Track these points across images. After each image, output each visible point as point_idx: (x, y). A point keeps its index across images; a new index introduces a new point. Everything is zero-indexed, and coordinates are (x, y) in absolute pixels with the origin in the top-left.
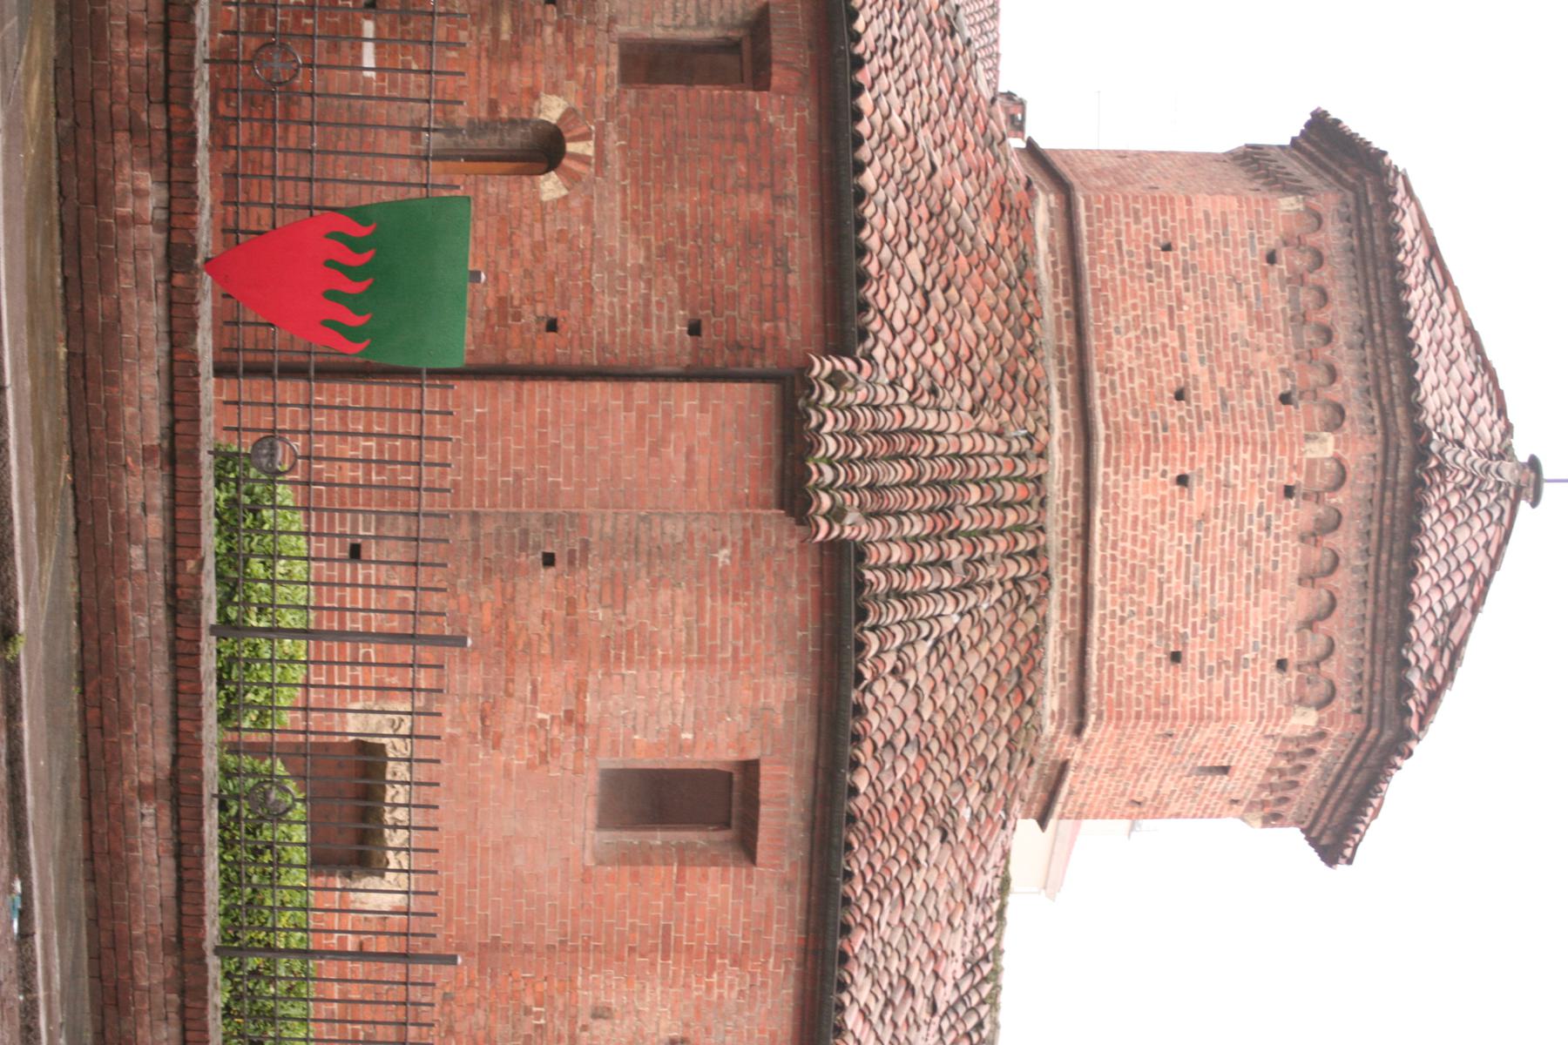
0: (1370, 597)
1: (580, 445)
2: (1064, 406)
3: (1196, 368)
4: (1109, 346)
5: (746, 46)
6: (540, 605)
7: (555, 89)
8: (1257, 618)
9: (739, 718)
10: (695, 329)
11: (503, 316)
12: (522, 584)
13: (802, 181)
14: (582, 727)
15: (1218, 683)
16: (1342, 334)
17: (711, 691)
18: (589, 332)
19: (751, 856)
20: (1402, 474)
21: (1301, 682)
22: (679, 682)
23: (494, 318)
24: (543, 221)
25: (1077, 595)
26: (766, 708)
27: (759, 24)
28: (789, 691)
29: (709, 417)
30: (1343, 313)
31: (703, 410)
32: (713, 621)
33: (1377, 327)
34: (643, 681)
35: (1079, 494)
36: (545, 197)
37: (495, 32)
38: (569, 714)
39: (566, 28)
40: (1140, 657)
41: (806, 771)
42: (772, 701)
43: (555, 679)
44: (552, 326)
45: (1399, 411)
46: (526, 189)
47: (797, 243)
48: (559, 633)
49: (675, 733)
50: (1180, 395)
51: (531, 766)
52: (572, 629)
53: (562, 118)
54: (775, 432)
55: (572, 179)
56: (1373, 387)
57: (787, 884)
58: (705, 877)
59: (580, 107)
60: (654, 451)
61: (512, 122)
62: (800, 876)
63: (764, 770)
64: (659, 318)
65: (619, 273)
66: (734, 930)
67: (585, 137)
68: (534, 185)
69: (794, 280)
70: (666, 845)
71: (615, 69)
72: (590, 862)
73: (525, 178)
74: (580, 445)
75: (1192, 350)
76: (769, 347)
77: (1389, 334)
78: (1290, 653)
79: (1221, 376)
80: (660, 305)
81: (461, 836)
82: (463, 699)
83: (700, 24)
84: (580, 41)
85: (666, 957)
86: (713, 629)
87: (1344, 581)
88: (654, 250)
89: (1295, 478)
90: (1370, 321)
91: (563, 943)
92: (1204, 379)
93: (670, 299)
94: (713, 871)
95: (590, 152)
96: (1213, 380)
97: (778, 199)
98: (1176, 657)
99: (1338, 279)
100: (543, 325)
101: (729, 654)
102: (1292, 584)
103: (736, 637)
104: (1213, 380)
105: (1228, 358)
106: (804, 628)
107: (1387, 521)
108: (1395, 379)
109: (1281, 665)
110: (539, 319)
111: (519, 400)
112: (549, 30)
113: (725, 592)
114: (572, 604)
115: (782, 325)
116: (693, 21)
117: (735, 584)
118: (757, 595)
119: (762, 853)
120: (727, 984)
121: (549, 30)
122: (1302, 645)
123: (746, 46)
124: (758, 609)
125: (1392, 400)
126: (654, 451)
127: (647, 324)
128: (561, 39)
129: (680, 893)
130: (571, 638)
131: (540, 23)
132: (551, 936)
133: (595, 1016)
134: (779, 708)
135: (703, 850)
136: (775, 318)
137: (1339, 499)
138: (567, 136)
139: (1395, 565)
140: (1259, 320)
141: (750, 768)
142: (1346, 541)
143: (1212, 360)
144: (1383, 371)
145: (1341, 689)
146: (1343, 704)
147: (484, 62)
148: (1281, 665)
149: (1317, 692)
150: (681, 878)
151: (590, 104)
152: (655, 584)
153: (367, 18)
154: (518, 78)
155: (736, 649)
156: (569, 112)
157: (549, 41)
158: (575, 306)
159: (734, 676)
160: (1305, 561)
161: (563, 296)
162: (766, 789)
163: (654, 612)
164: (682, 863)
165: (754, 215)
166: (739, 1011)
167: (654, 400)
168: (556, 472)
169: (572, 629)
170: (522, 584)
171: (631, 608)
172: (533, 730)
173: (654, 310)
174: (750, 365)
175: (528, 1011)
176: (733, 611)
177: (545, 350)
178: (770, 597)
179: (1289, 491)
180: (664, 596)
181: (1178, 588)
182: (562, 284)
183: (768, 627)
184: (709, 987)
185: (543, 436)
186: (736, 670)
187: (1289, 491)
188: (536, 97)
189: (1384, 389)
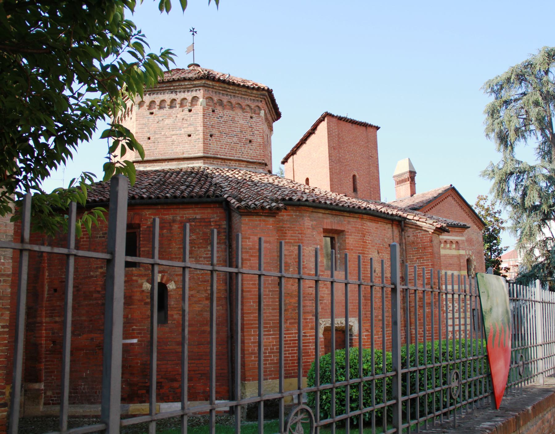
0: (237, 95)
2: (193, 163)
3: (182, 131)
4: (177, 153)
6: (289, 286)
7: (141, 286)
8: (241, 122)
9: (314, 233)
13: (168, 214)
15: (256, 132)
16: (173, 96)
17: (309, 240)
19: (343, 231)
20: (211, 83)
21: (255, 113)
22: (307, 249)
25: (237, 163)
28: (308, 220)
29: (251, 237)
31: (249, 238)
32: (292, 239)
33: (172, 88)
35: (215, 160)
36: (175, 287)
40: (251, 149)
41: (325, 216)
42: (310, 224)
45: (195, 83)
46: (172, 293)
47: (187, 216)
50: (190, 136)
54: (254, 218)
55: (169, 281)
56: (188, 90)
57: (349, 222)
58: (348, 243)
59: (146, 278)
62: (347, 219)
63: (325, 227)
66: (358, 236)
69: (198, 217)
71: (134, 269)
73: (169, 293)
75: (178, 132)
76: (218, 223)
77: (174, 85)
78: (249, 115)
79: (184, 126)
85: (364, 253)
86: (293, 239)
87: (234, 101)
89: (210, 109)
90: (170, 89)
92: (186, 129)
93: (205, 251)
94: (347, 241)
96: (186, 127)
97: (174, 221)
98: (250, 141)
102: (234, 113)
103: (296, 233)
104: (186, 127)
105: (179, 124)
106: (292, 215)
107: (221, 89)
108: (186, 83)
109: (251, 117)
113: (284, 236)
117: (282, 233)
118: (285, 227)
119: (343, 229)
120: (368, 238)
122: (247, 112)
124: (288, 227)
125: (192, 85)
129: (352, 250)
134: (312, 223)
135: (341, 244)
136: (210, 222)
137: (215, 99)
140: (169, 116)
142: (225, 99)
143: (180, 128)
144: (184, 87)
145: (257, 104)
146: (260, 104)
147: (132, 307)
148: (251, 117)
150: (348, 249)
151: (145, 275)
155: (299, 233)
159: (305, 234)
160: (229, 109)
161: (205, 282)
162: (329, 227)
163: (290, 255)
164: (346, 249)
165: (179, 228)
166: (372, 236)
174: (225, 228)
176: (289, 233)
178: (285, 224)
179: (213, 111)
181: (235, 139)
182: (202, 282)
183: (293, 225)
184: (369, 243)
187: (213, 111)
188: (143, 291)
189: (189, 86)
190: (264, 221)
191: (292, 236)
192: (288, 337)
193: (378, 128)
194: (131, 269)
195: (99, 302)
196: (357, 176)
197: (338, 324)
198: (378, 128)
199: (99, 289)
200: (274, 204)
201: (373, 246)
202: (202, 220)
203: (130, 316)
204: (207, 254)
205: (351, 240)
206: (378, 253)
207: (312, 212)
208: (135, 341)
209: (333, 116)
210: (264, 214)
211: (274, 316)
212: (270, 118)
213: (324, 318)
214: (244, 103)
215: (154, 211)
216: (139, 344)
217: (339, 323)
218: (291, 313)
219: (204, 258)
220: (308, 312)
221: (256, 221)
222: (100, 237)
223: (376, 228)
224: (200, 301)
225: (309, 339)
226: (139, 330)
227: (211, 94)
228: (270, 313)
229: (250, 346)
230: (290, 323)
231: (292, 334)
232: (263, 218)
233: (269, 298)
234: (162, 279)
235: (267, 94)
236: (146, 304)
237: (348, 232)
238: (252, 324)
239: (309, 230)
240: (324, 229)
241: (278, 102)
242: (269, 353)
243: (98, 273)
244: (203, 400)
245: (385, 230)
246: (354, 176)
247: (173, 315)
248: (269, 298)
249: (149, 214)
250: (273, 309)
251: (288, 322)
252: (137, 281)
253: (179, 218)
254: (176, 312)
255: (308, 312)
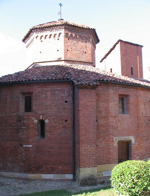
0: (79, 32)
1: (88, 117)
5: (26, 95)
7: (33, 121)
10: (66, 102)
11: (66, 127)
12: (100, 124)
14: (116, 116)
16: (51, 33)
18: (67, 116)
19: (128, 95)
20: (67, 27)
23: (65, 129)
24: (52, 122)
26: (113, 93)
27: (23, 94)
30: (48, 33)
34: (110, 108)
35: (69, 62)
36: (48, 122)
37: (25, 129)
38: (115, 118)
39: (24, 119)
43: (111, 120)
44: (66, 121)
46: (47, 125)
48: (105, 119)
49: (116, 104)
51: (120, 122)
52: (105, 118)
53: (37, 120)
54: (85, 90)
55: (46, 119)
57: (131, 91)
59: (35, 117)
60: (88, 107)
61: (38, 126)
63: (120, 93)
64: (65, 106)
65: (59, 112)
67: (40, 117)
68: (47, 123)
69: (59, 89)
70: (126, 106)
71: (30, 113)
72: (129, 115)
74: (88, 117)
78: (85, 41)
80: (63, 106)
81: (127, 131)
82: (113, 131)
83: (23, 102)
84: (26, 118)
85: (138, 106)
88: (56, 107)
91: (137, 118)
94: (130, 100)
95: (42, 116)
99: (44, 34)
100: (66, 122)
101: (107, 97)
110: (65, 122)
111: (82, 125)
112: (24, 122)
114: (102, 118)
115: (65, 90)
116: (22, 103)
119: (128, 94)
120: (140, 99)
121: (24, 122)
122: (84, 40)
123: (26, 95)
124: (102, 94)
126: (88, 107)
127: (66, 108)
128: (25, 120)
130: (106, 118)
131: (23, 123)
132: (136, 119)
133: (142, 114)
135: (127, 101)
136: (65, 91)
138: (39, 119)
139: (76, 29)
141: (120, 95)
146: (90, 36)
147: (29, 130)
149: (89, 39)
151: (35, 116)
152: (100, 107)
153: (23, 146)
154: (31, 126)
155: (107, 97)
156: (36, 119)
157: (26, 122)
158: (63, 118)
165: (50, 94)
167: (82, 107)
168: (92, 120)
169: (105, 118)
170: (100, 124)
171: (102, 110)
172: (116, 122)
173: (64, 107)
175: (142, 122)
177: (70, 122)
180: (101, 106)
183: (104, 92)
185: (87, 122)
186: (110, 97)
188: (34, 123)
190: (90, 91)
191: (103, 98)
192: (101, 146)
193: (142, 46)
194: (29, 113)
195: (15, 128)
196: (133, 68)
197: (125, 139)
198: (142, 46)
199: (15, 122)
200: (95, 83)
201: (142, 102)
202: (61, 90)
203: (28, 134)
204: (63, 106)
205: (132, 99)
206: (144, 105)
207: (113, 86)
208: (31, 146)
209: (123, 41)
210: (90, 88)
211: (95, 137)
212: (94, 42)
213: (118, 137)
214: (83, 35)
215: (39, 86)
216: (32, 147)
217: (125, 139)
218: (103, 134)
219: (62, 108)
220: (111, 134)
221: (86, 91)
222: (15, 98)
223: (144, 93)
224: (60, 128)
225: (111, 147)
226: (33, 141)
227: (67, 32)
228: (92, 136)
229: (83, 152)
230: (102, 139)
231: (103, 144)
232: (89, 90)
233: (92, 129)
234: (42, 118)
235: (93, 31)
236: (36, 129)
237: (130, 95)
238: (83, 141)
239: (112, 95)
240: (119, 94)
241: (98, 35)
242: (92, 155)
243: (14, 115)
244: (61, 174)
245: (147, 94)
246: (132, 68)
247: (47, 135)
248: (92, 129)
249: (37, 88)
250: (94, 134)
251: (101, 138)
252: (31, 119)
253: (50, 89)
254: (49, 133)
255: (111, 134)
